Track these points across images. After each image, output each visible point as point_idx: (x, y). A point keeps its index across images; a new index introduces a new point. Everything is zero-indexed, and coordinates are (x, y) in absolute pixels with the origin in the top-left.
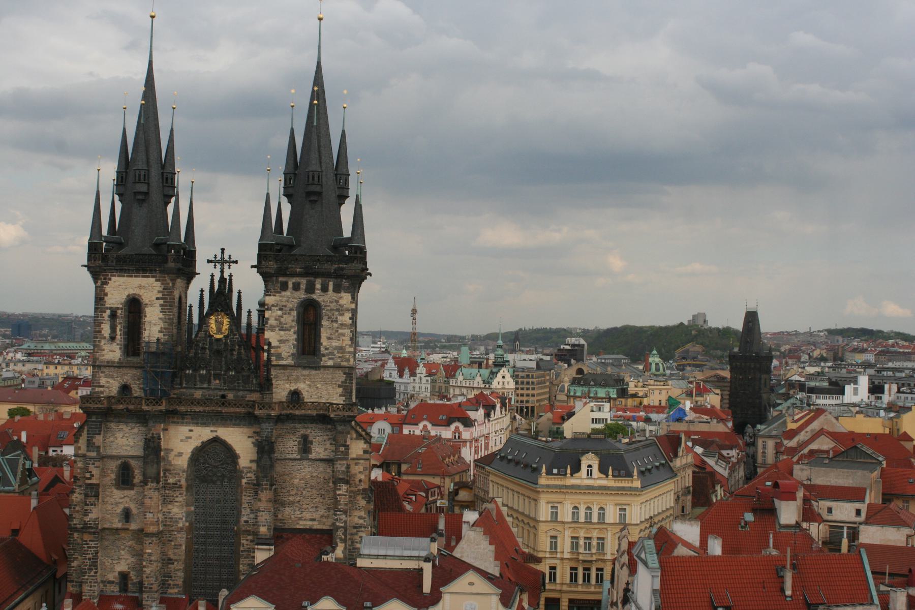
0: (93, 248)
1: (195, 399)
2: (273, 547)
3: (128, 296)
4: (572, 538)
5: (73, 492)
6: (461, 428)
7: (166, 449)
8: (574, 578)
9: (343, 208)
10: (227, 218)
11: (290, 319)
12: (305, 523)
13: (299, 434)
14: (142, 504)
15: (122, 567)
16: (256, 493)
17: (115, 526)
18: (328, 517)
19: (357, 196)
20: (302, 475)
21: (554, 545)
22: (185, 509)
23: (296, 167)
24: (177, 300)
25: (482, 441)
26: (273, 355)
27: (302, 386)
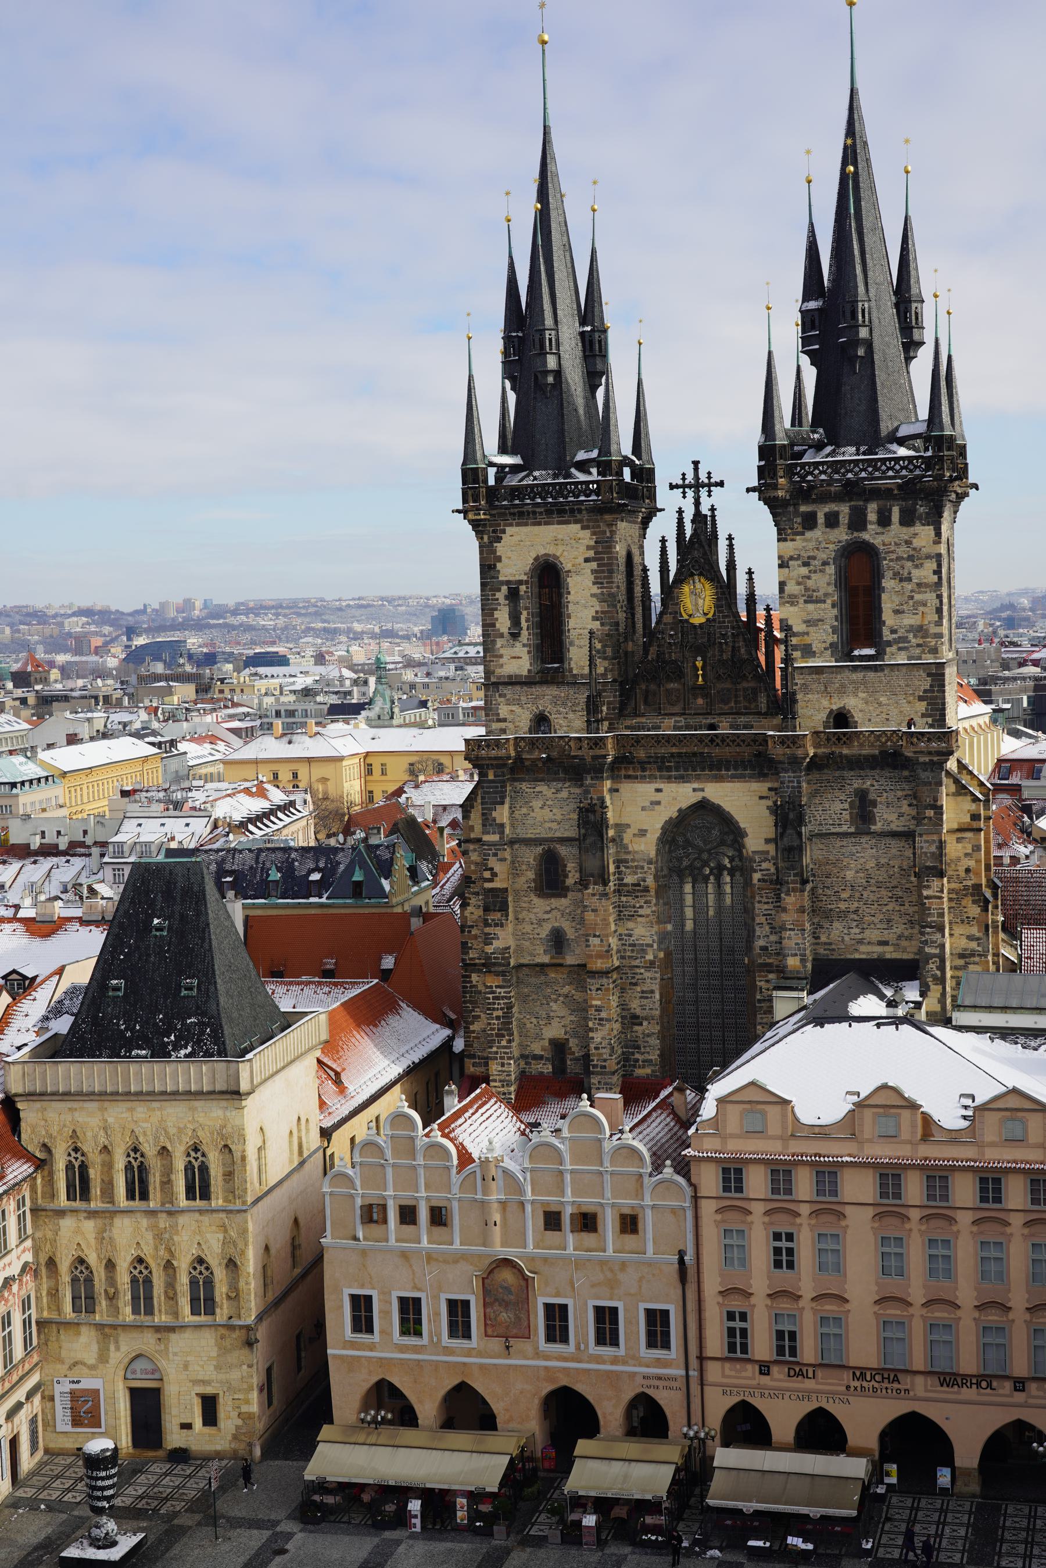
3: (536, 559)
7: (617, 825)
9: (914, 364)
11: (824, 581)
14: (582, 919)
15: (554, 1031)
16: (779, 899)
17: (539, 960)
18: (909, 938)
19: (937, 340)
20: (860, 864)
22: (656, 928)
26: (795, 648)
27: (853, 703)
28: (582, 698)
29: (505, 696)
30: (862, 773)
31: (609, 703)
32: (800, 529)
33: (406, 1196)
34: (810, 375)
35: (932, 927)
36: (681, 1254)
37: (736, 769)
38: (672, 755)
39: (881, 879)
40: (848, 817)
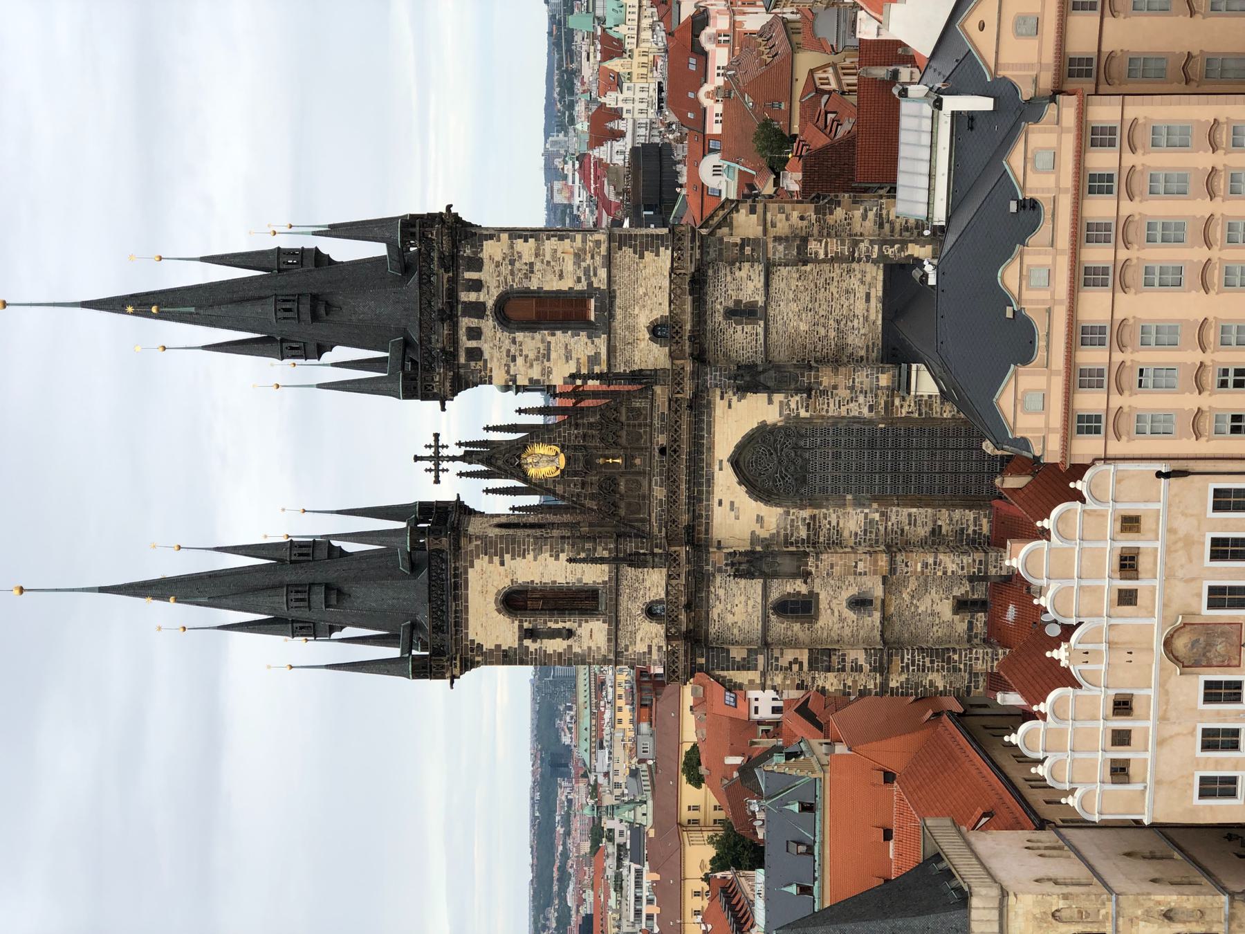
0: (422, 670)
3: (499, 611)
5: (823, 691)
6: (709, 31)
7: (752, 543)
9: (336, 257)
11: (530, 342)
13: (724, 325)
18: (864, 273)
19: (315, 234)
23: (268, 340)
24: (504, 532)
27: (644, 319)
28: (629, 572)
29: (627, 646)
31: (637, 547)
32: (481, 363)
33: (1103, 739)
34: (341, 353)
35: (854, 252)
36: (1159, 474)
37: (702, 430)
38: (689, 489)
39: (808, 298)
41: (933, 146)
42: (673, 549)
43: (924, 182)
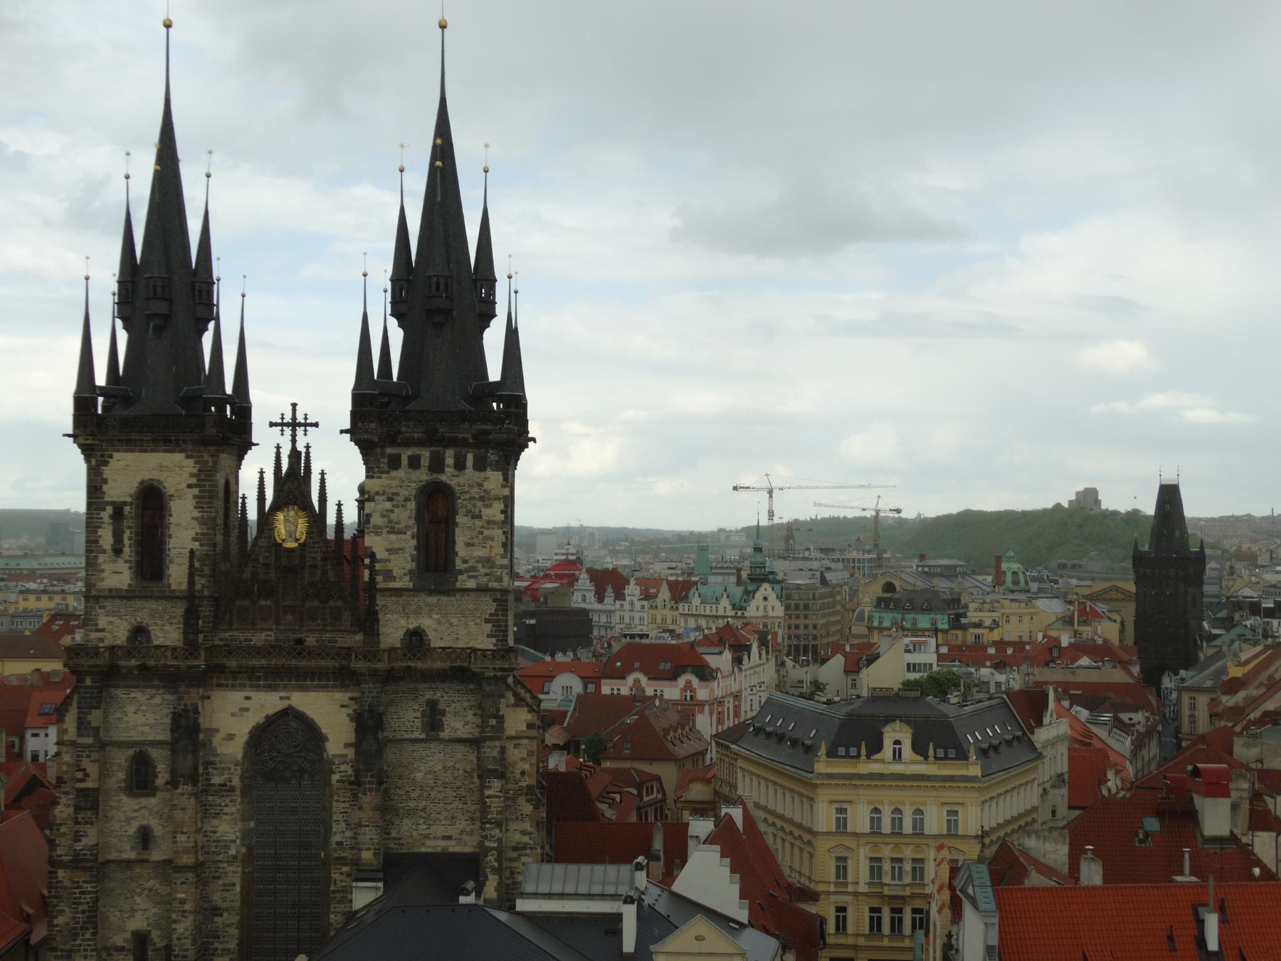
1: (254, 647)
2: (380, 885)
3: (142, 482)
4: (872, 859)
5: (55, 803)
6: (695, 682)
8: (875, 924)
9: (487, 334)
10: (300, 354)
11: (406, 515)
12: (435, 843)
13: (422, 700)
15: (138, 923)
16: (355, 797)
17: (125, 856)
18: (470, 833)
21: (841, 871)
22: (240, 825)
24: (221, 488)
25: (730, 704)
26: (378, 573)
27: (426, 622)
28: (180, 609)
30: (433, 685)
32: (386, 468)
37: (320, 680)
38: (262, 667)
40: (420, 725)
41: (590, 896)
42: (203, 653)
43: (557, 889)
